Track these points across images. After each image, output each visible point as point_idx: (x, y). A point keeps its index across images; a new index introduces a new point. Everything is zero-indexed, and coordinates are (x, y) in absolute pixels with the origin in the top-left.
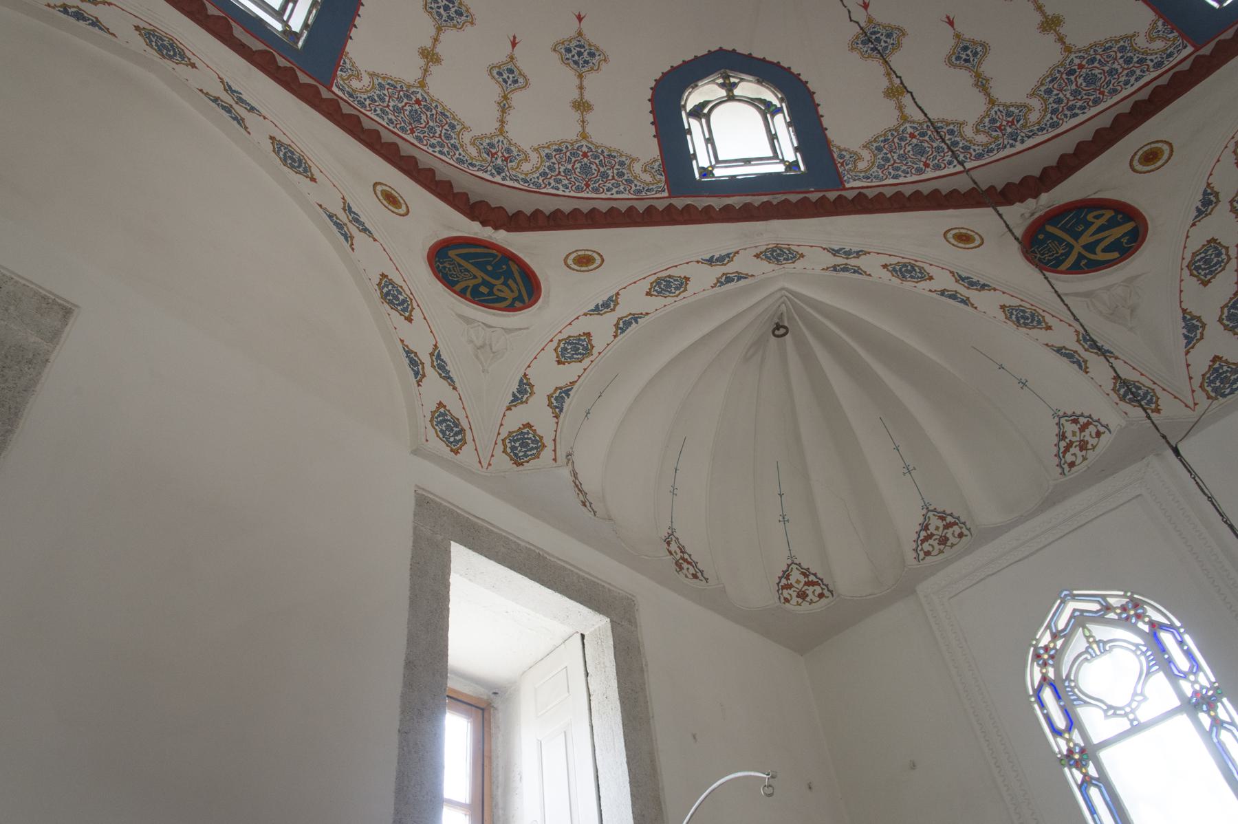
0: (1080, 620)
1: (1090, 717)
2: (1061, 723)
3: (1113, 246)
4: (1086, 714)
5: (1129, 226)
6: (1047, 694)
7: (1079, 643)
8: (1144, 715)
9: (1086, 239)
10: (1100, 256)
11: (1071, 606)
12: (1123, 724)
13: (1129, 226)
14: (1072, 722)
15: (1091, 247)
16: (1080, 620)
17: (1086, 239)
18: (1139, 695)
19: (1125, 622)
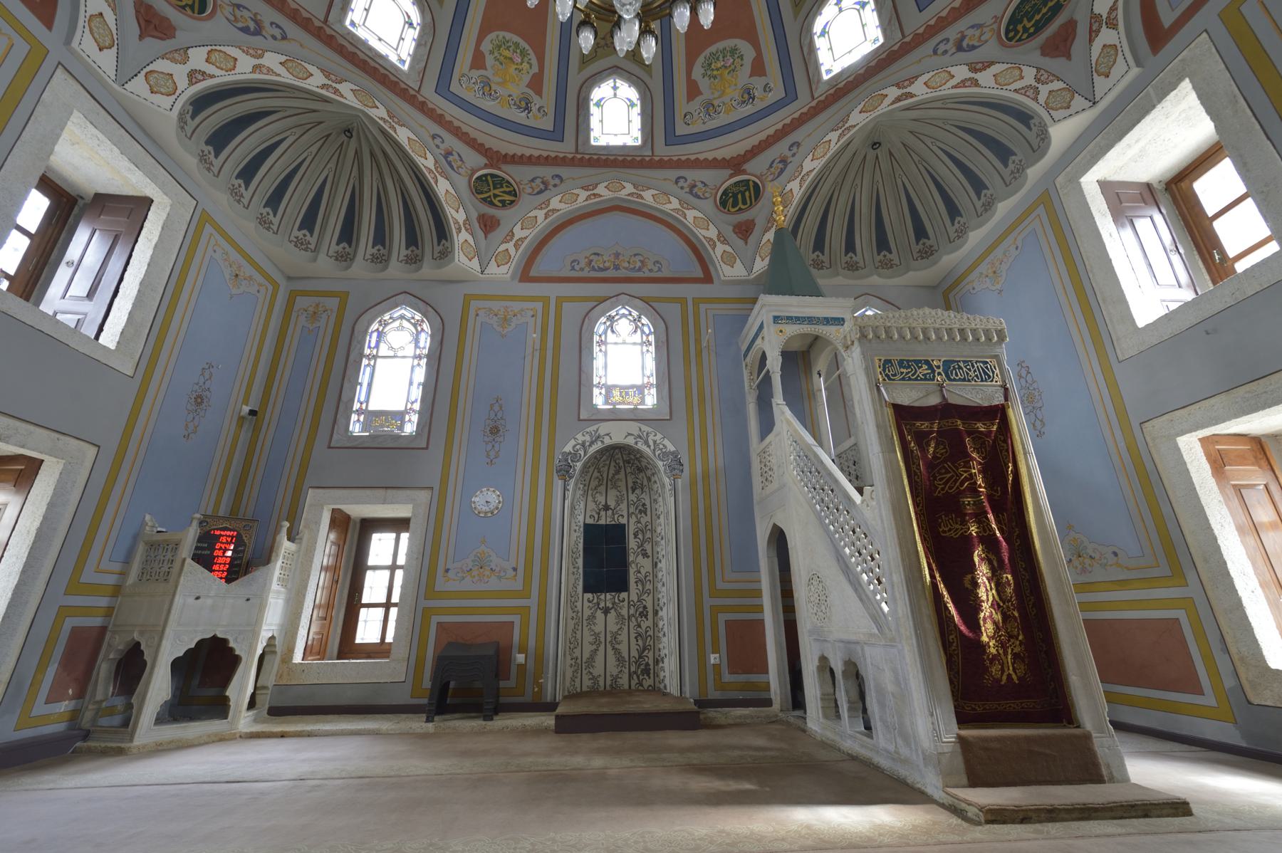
0: (402, 317)
1: (383, 347)
2: (373, 345)
3: (503, 202)
4: (382, 345)
5: (512, 198)
6: (375, 335)
7: (397, 324)
8: (399, 354)
9: (497, 192)
10: (496, 201)
11: (403, 311)
12: (391, 353)
13: (512, 198)
14: (377, 346)
15: (496, 196)
16: (402, 317)
17: (497, 192)
18: (402, 348)
19: (415, 325)
